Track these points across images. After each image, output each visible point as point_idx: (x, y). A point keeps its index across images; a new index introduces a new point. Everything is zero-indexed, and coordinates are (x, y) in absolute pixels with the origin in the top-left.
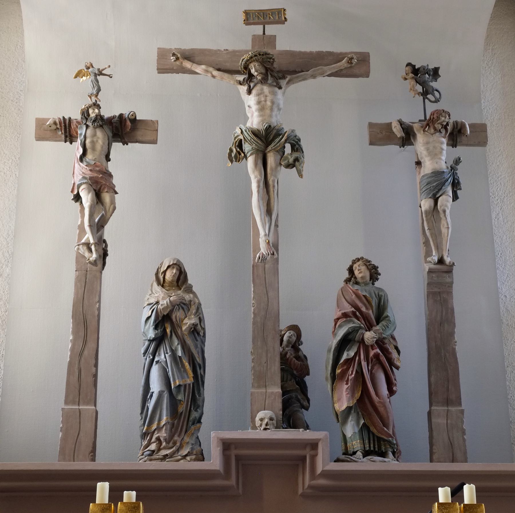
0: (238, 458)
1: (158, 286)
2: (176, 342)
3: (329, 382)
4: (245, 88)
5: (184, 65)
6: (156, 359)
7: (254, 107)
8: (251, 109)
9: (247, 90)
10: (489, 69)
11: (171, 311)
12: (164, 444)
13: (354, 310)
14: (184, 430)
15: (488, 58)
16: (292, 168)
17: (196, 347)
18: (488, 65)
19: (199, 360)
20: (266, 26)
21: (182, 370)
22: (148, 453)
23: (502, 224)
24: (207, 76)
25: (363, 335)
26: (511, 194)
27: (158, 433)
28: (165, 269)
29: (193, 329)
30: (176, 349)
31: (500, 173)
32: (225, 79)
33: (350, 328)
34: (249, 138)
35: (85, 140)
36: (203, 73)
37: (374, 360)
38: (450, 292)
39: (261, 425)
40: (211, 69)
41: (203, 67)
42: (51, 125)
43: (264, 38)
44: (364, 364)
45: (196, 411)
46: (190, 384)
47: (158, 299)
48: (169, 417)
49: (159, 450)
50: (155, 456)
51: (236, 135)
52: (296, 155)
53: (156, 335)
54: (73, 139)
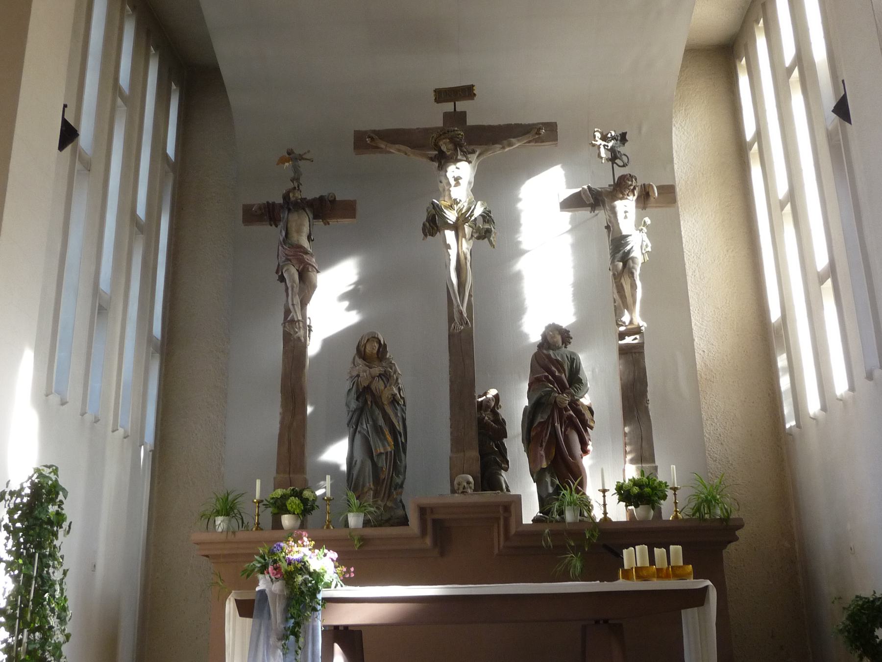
1: (360, 358)
4: (436, 164)
6: (359, 429)
10: (683, 130)
11: (371, 383)
13: (546, 374)
14: (387, 495)
15: (681, 119)
16: (484, 239)
17: (396, 415)
18: (681, 125)
19: (400, 428)
20: (456, 103)
21: (383, 437)
23: (699, 280)
26: (707, 251)
31: (696, 230)
37: (567, 422)
38: (642, 352)
39: (458, 489)
44: (557, 425)
45: (398, 476)
46: (391, 452)
52: (487, 226)
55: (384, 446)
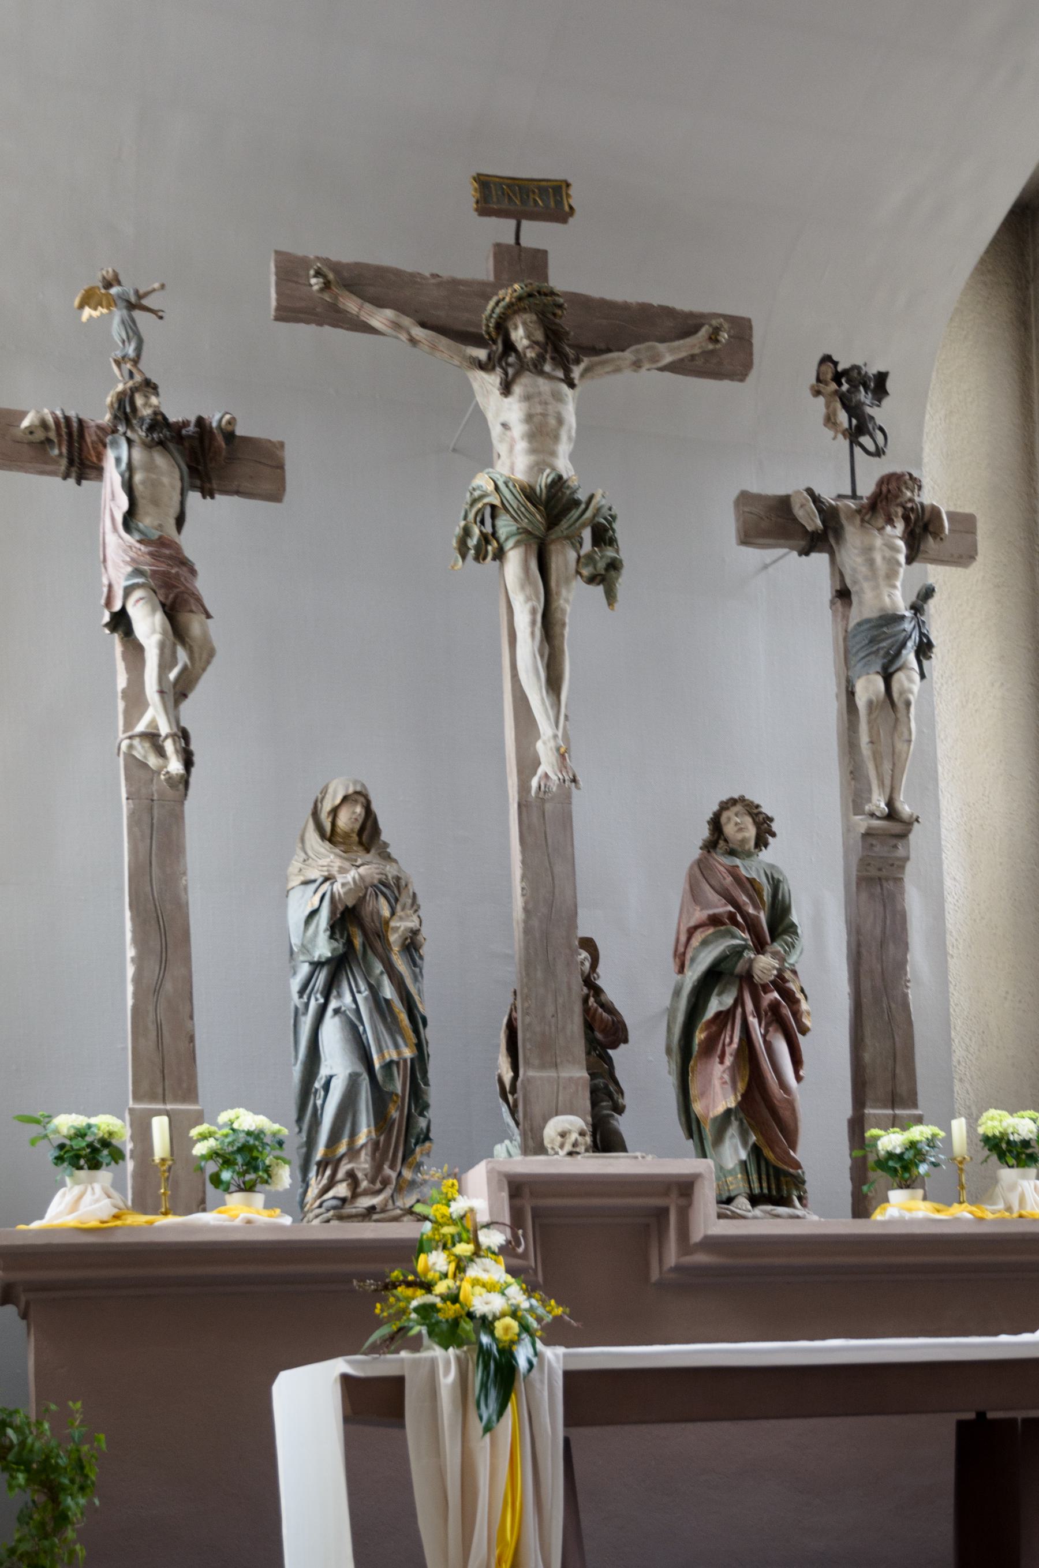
0: (536, 1213)
2: (378, 968)
3: (674, 1058)
5: (341, 306)
6: (333, 1004)
7: (518, 429)
8: (508, 433)
9: (501, 384)
12: (364, 1184)
22: (334, 1202)
24: (397, 338)
25: (751, 961)
27: (350, 1162)
28: (338, 801)
29: (409, 940)
30: (379, 984)
32: (443, 352)
33: (728, 946)
34: (515, 505)
35: (131, 478)
36: (389, 331)
40: (406, 321)
41: (389, 313)
42: (33, 429)
43: (520, 255)
44: (753, 1021)
47: (328, 871)
48: (373, 1128)
49: (355, 1195)
50: (348, 1210)
51: (477, 494)
53: (333, 950)
54: (88, 471)
55: (397, 1046)
